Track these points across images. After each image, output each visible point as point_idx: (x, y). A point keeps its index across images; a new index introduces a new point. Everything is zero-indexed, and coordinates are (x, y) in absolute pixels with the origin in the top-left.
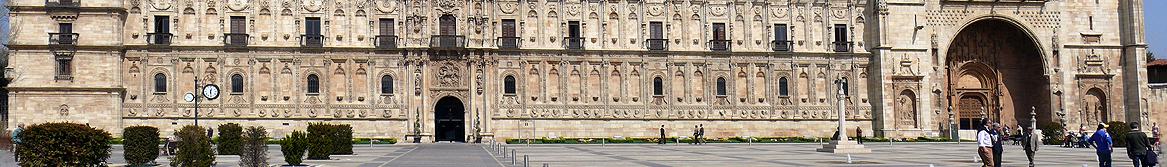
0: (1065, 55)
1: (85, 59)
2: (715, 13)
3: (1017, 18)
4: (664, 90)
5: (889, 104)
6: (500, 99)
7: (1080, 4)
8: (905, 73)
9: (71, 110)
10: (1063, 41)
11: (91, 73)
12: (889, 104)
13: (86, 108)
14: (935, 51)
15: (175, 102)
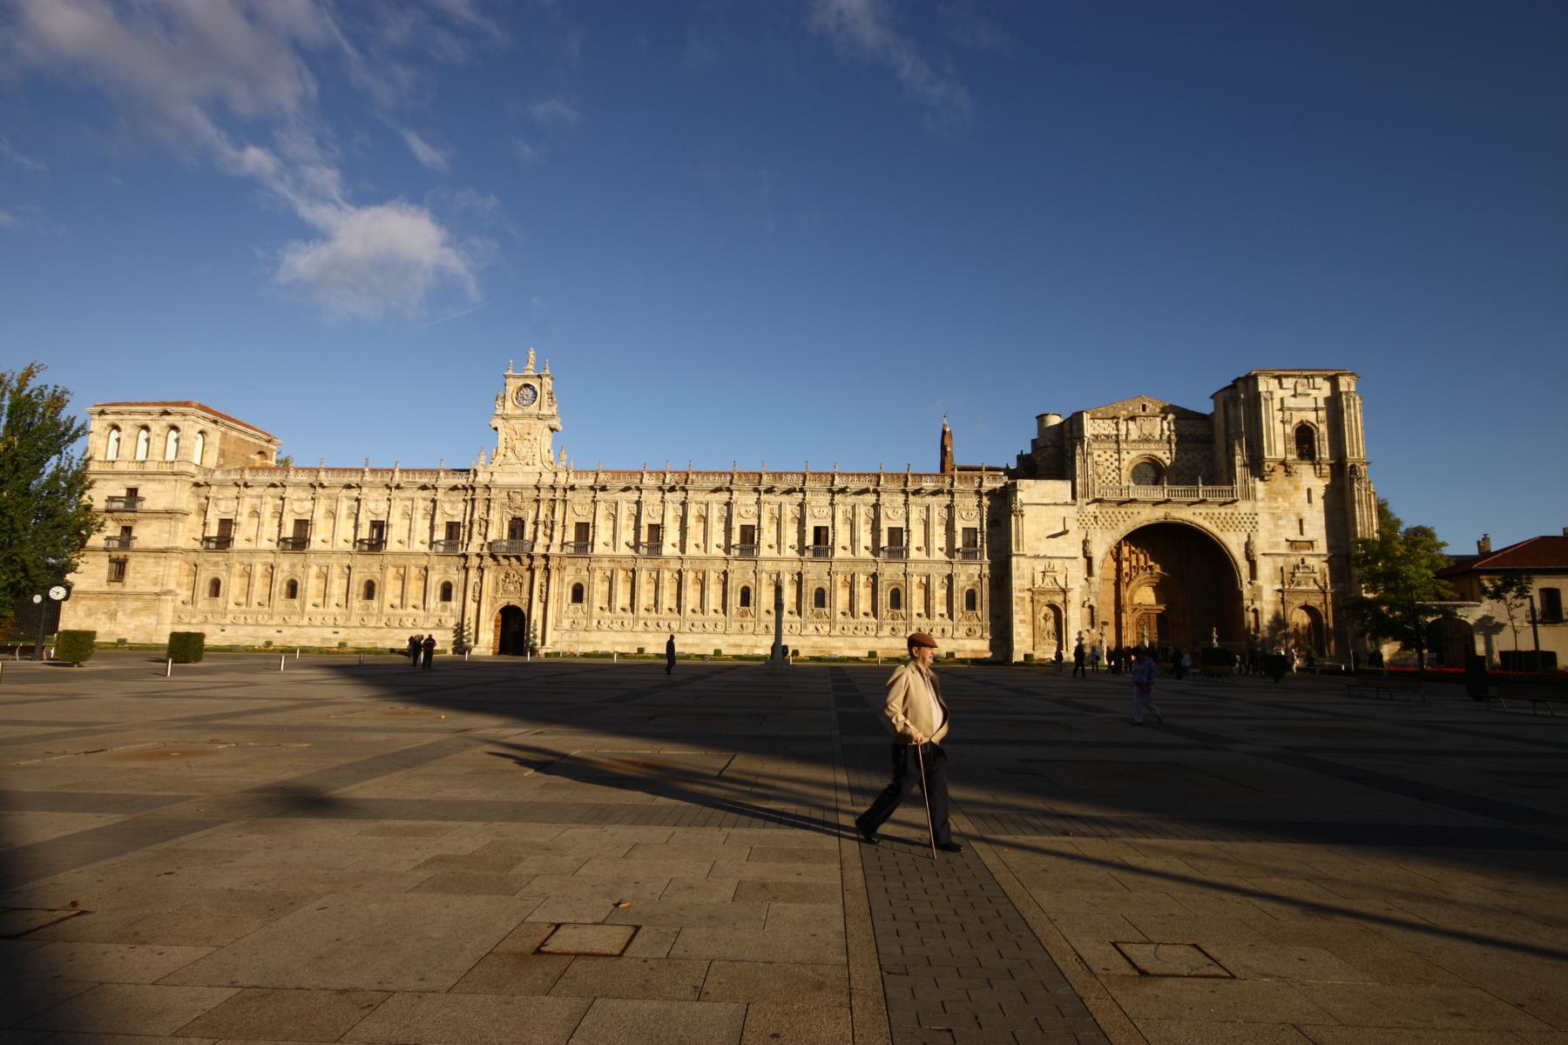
0: (1265, 568)
1: (139, 562)
2: (817, 515)
3: (1199, 521)
4: (752, 601)
5: (1022, 621)
6: (565, 608)
7: (1286, 504)
8: (1048, 584)
9: (120, 614)
10: (1261, 545)
11: (144, 577)
12: (1022, 621)
13: (135, 612)
14: (1089, 560)
15: (226, 608)
